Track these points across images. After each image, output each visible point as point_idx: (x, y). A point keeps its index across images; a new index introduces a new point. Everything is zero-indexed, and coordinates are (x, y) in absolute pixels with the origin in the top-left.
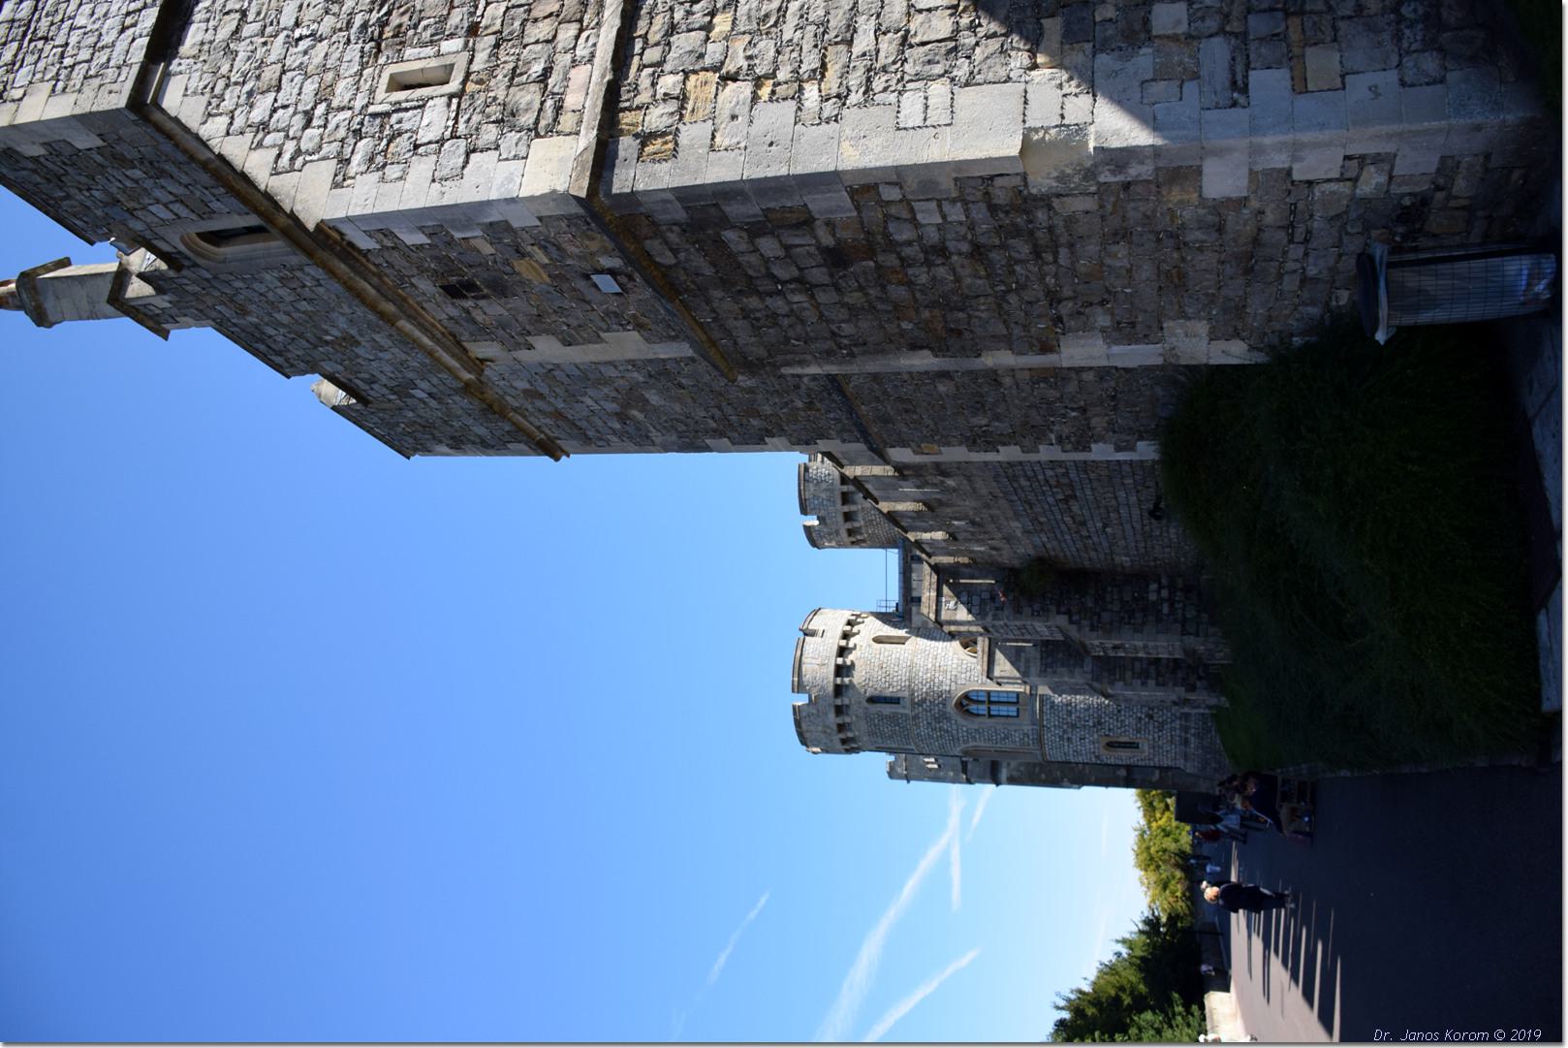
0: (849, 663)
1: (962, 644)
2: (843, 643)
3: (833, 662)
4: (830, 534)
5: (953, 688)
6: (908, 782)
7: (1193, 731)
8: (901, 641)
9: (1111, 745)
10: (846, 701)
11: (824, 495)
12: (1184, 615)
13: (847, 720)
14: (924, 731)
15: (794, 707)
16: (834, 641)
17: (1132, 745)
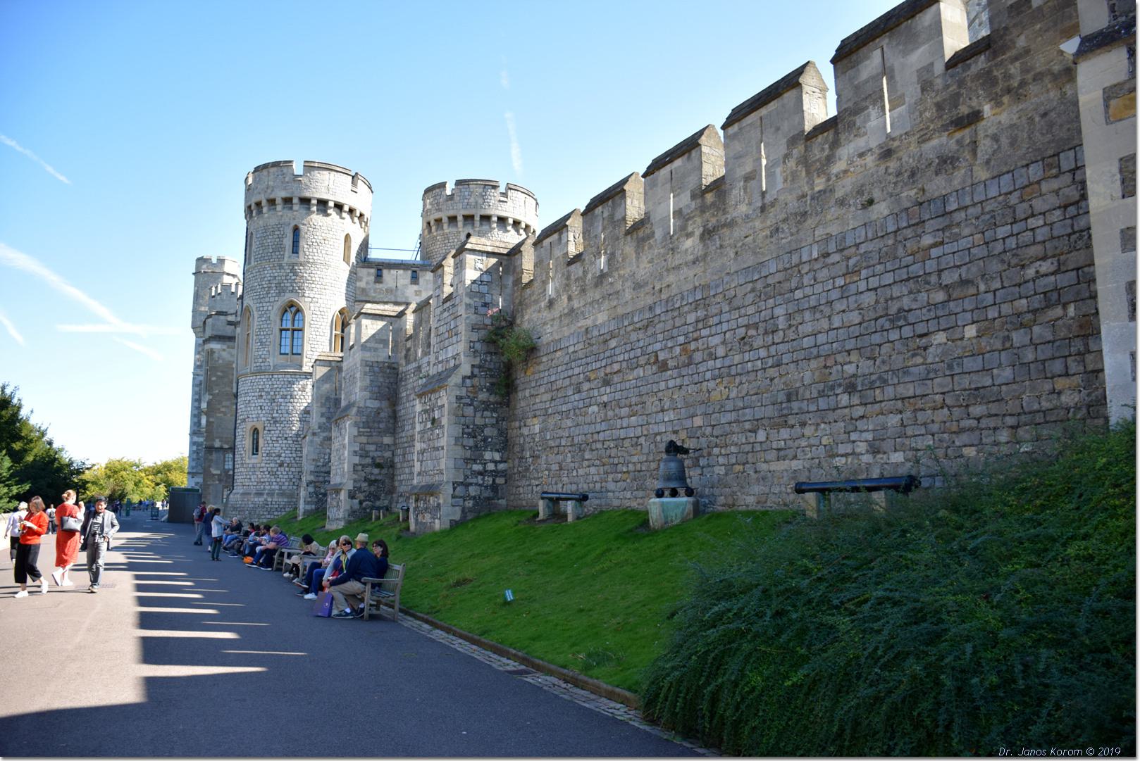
0: (329, 211)
1: (343, 308)
2: (346, 208)
3: (332, 198)
4: (438, 204)
5: (306, 299)
6: (194, 274)
7: (269, 499)
8: (346, 258)
9: (256, 431)
10: (296, 207)
11: (472, 200)
12: (471, 484)
13: (279, 208)
14: (268, 273)
15: (291, 162)
16: (348, 201)
17: (256, 449)
